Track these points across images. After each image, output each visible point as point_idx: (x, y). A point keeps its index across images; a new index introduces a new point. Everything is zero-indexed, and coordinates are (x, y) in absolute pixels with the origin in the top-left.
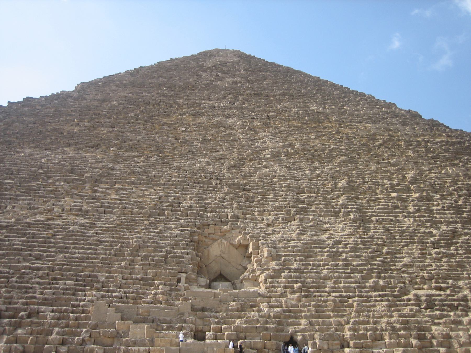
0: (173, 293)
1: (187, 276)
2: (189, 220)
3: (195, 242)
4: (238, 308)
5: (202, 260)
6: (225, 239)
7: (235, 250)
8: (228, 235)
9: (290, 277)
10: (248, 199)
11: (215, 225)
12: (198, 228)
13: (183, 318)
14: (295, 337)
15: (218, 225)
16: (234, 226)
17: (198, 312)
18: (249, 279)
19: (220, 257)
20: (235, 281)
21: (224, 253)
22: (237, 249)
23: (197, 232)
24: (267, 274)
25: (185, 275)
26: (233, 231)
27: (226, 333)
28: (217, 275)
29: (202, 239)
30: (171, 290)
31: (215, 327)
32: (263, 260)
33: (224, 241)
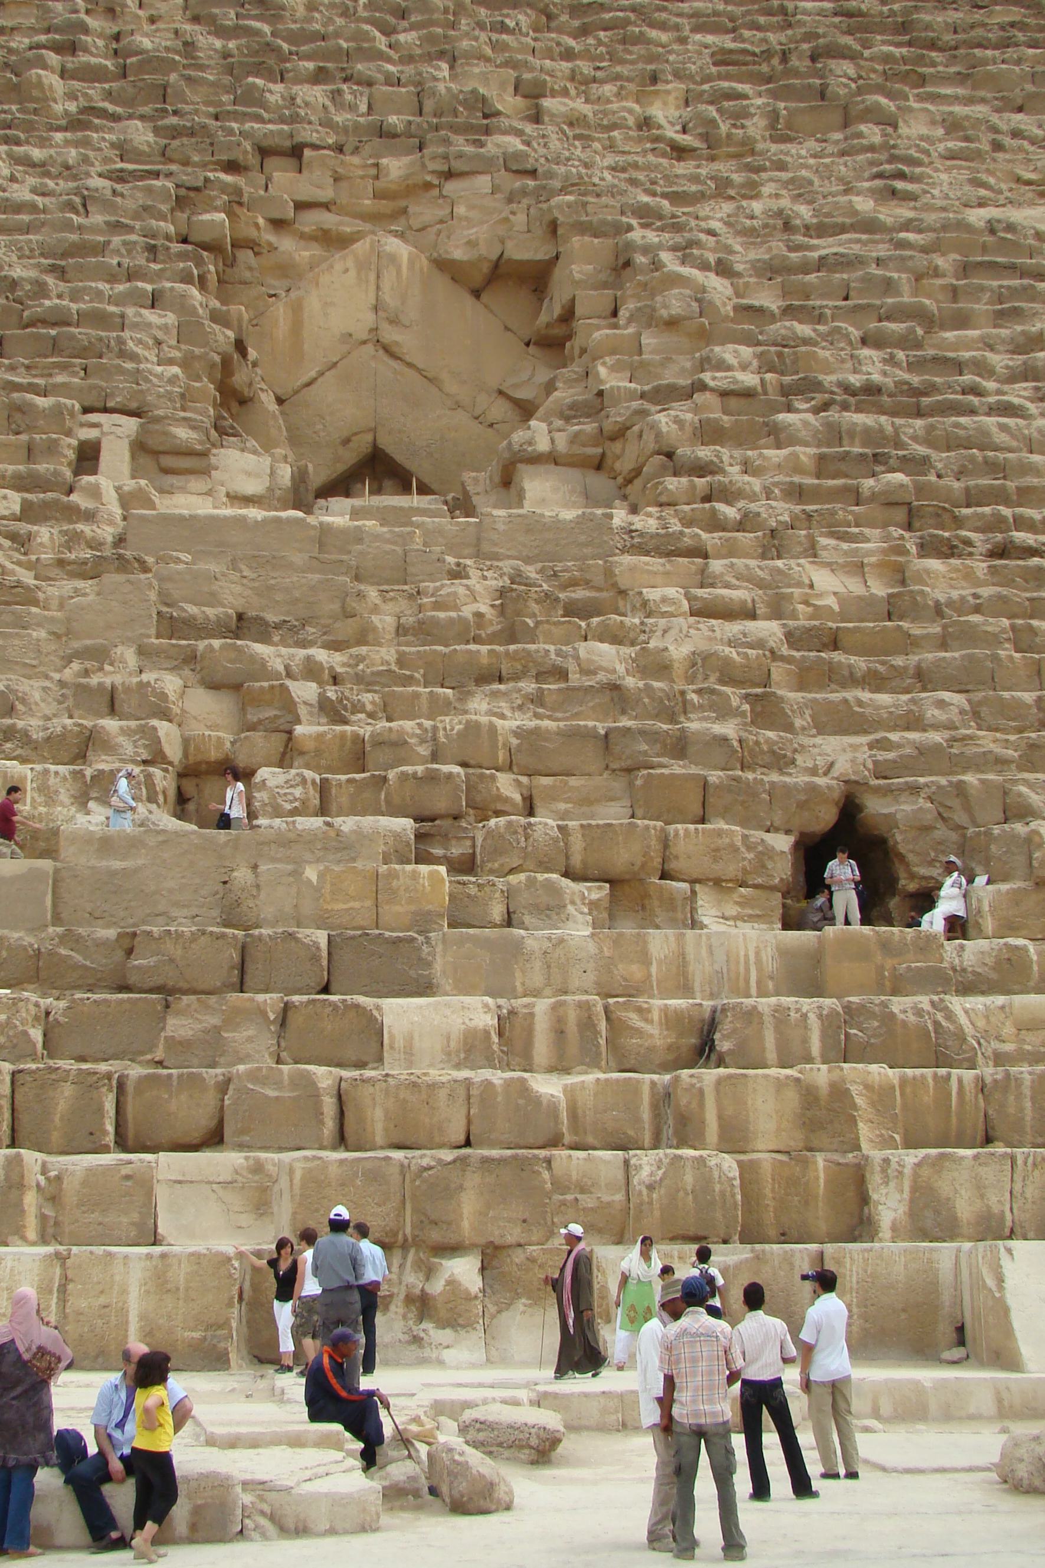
0: (45, 534)
1: (143, 429)
2: (174, 120)
3: (205, 247)
4: (479, 615)
5: (252, 354)
6: (401, 235)
7: (469, 300)
9: (835, 434)
10: (550, 17)
11: (340, 149)
12: (232, 167)
13: (94, 680)
14: (875, 807)
15: (356, 150)
16: (460, 156)
17: (201, 645)
18: (552, 459)
19: (370, 348)
20: (468, 476)
21: (394, 321)
22: (477, 294)
23: (224, 188)
24: (677, 421)
25: (130, 425)
26: (451, 187)
27: (391, 775)
28: (350, 457)
29: (253, 233)
30: (28, 513)
31: (320, 736)
32: (648, 340)
33: (393, 245)
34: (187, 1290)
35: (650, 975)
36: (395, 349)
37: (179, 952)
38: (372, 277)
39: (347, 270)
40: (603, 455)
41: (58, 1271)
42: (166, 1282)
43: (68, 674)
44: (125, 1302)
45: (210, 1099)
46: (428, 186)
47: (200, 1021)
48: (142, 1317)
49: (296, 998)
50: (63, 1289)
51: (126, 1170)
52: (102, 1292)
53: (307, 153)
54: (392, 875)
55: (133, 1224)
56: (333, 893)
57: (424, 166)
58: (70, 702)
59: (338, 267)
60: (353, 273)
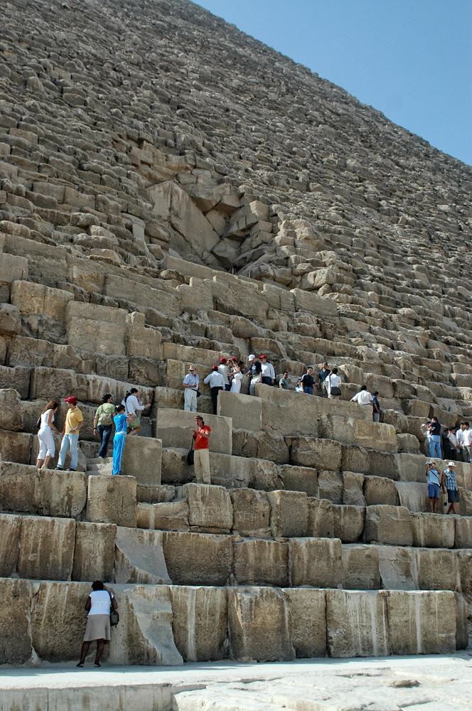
8: (185, 178)
21: (177, 216)
22: (205, 214)
26: (195, 171)
34: (439, 612)
35: (464, 481)
36: (176, 226)
37: (320, 449)
38: (169, 196)
39: (160, 192)
40: (292, 281)
41: (383, 603)
42: (430, 608)
43: (186, 316)
44: (414, 619)
45: (360, 518)
46: (187, 169)
47: (332, 484)
48: (422, 627)
49: (369, 476)
50: (387, 613)
51: (367, 552)
52: (405, 614)
53: (145, 142)
54: (378, 427)
55: (372, 579)
56: (359, 431)
57: (186, 161)
58: (189, 330)
59: (157, 189)
60: (162, 193)
